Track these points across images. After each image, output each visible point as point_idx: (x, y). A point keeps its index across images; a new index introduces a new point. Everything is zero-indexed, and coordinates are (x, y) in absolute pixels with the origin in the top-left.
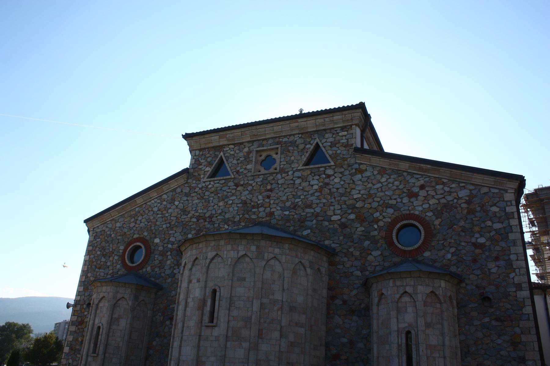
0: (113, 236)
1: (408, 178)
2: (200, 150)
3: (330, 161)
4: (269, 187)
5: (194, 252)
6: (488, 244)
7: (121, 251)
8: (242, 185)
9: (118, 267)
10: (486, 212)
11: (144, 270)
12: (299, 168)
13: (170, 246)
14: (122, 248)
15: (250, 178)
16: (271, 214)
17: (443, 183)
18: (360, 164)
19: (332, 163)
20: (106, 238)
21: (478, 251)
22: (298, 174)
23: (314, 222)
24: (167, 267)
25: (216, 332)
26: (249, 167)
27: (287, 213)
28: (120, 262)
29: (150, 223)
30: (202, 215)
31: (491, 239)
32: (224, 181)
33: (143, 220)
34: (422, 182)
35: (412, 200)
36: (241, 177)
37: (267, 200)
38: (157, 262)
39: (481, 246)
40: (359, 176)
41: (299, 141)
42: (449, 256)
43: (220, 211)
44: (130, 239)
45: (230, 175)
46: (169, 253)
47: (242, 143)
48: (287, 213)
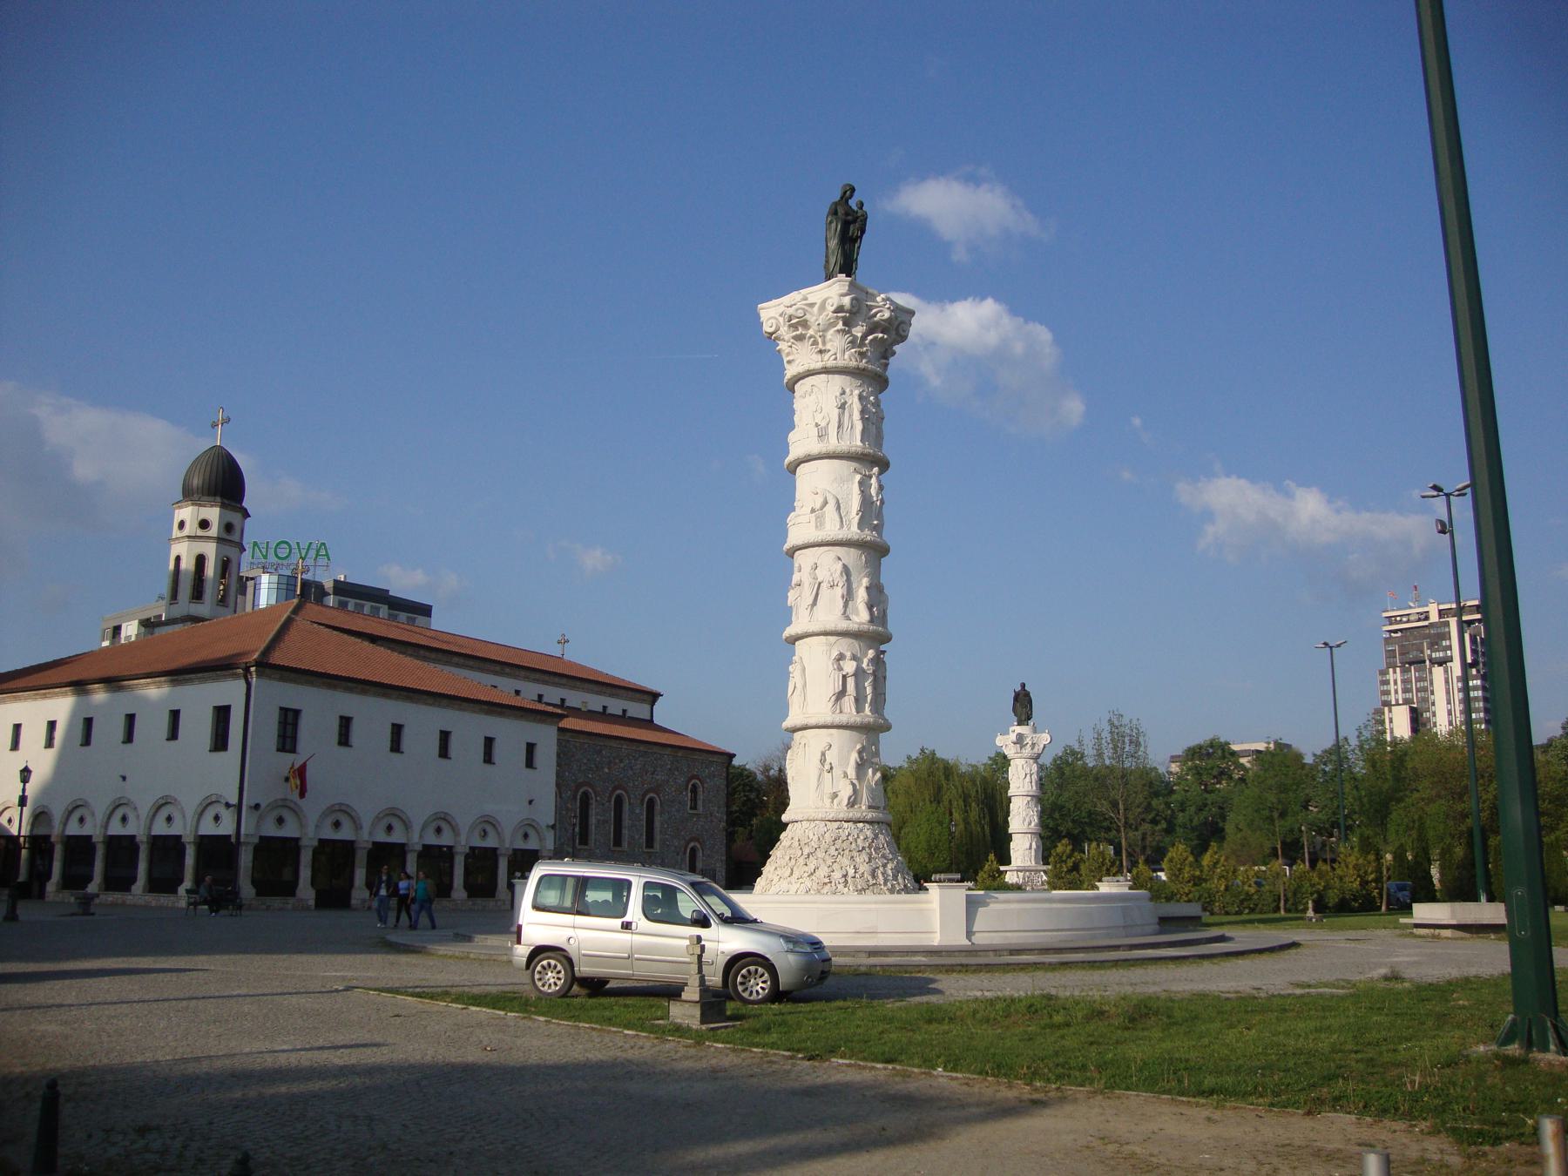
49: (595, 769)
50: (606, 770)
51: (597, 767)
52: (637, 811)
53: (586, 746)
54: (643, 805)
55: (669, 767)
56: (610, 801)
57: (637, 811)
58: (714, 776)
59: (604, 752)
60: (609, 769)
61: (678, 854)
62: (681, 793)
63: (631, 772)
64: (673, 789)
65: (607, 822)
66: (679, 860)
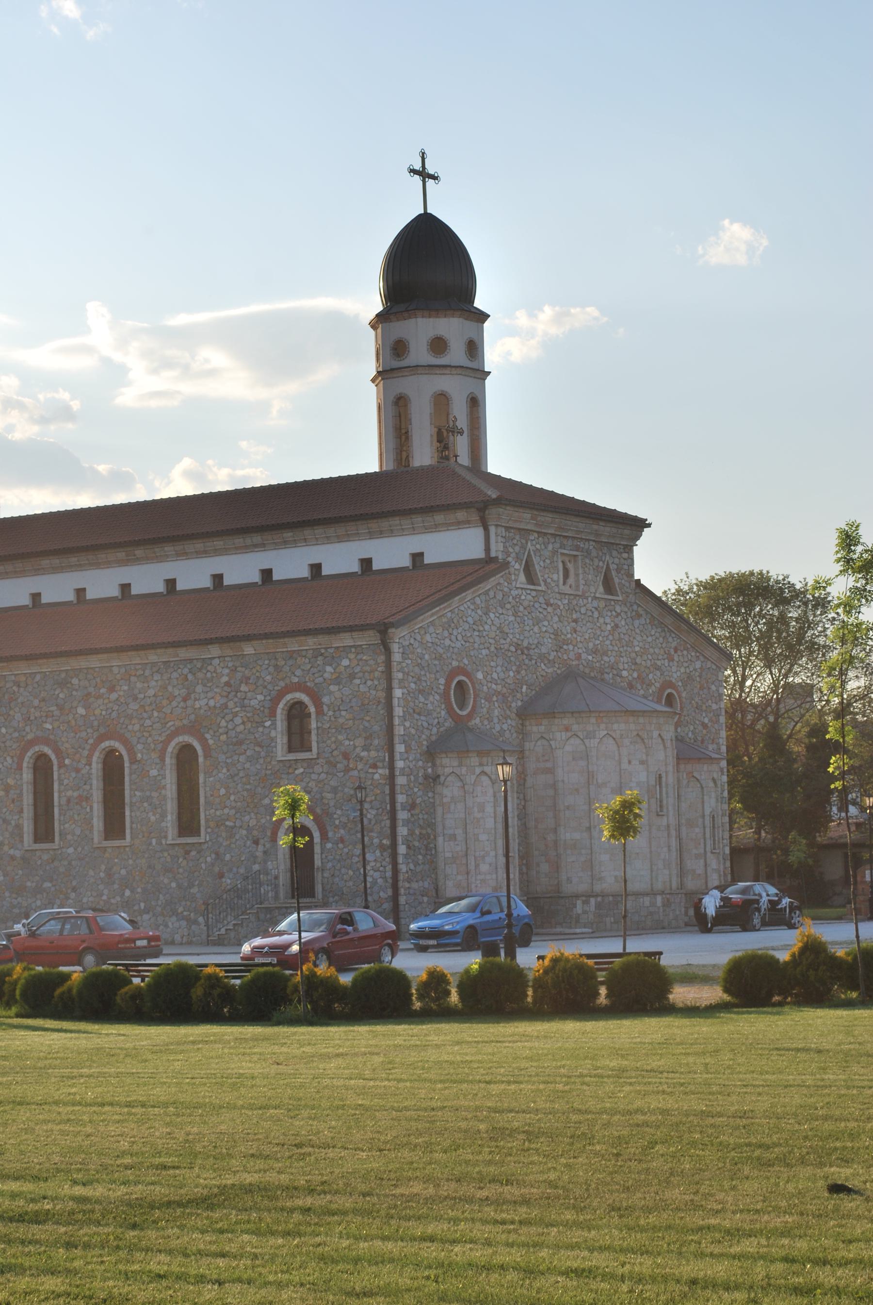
0: (427, 657)
1: (668, 634)
2: (507, 528)
3: (619, 594)
4: (574, 616)
5: (632, 727)
6: (709, 725)
7: (442, 687)
8: (551, 605)
9: (443, 713)
10: (709, 688)
11: (473, 722)
12: (597, 595)
13: (494, 686)
14: (442, 681)
15: (558, 596)
16: (579, 657)
17: (687, 649)
18: (639, 606)
19: (620, 598)
20: (419, 661)
21: (704, 732)
22: (595, 604)
23: (611, 675)
24: (496, 720)
25: (664, 821)
26: (555, 577)
27: (590, 658)
28: (443, 706)
29: (468, 644)
30: (520, 643)
31: (711, 720)
32: (534, 594)
33: (460, 637)
34: (674, 644)
35: (671, 664)
36: (549, 592)
37: (575, 635)
38: (485, 710)
39: (705, 726)
40: (637, 623)
41: (594, 553)
42: (690, 735)
43: (536, 642)
44: (450, 667)
45: (540, 585)
46: (495, 699)
47: (545, 534)
48: (590, 658)
49: (57, 713)
50: (81, 711)
51: (61, 708)
52: (154, 772)
53: (38, 678)
54: (162, 759)
55: (225, 679)
56: (90, 764)
57: (154, 772)
58: (352, 676)
59: (75, 681)
60: (87, 708)
61: (256, 842)
62: (261, 724)
63: (134, 706)
64: (238, 720)
65: (87, 799)
66: (259, 854)
